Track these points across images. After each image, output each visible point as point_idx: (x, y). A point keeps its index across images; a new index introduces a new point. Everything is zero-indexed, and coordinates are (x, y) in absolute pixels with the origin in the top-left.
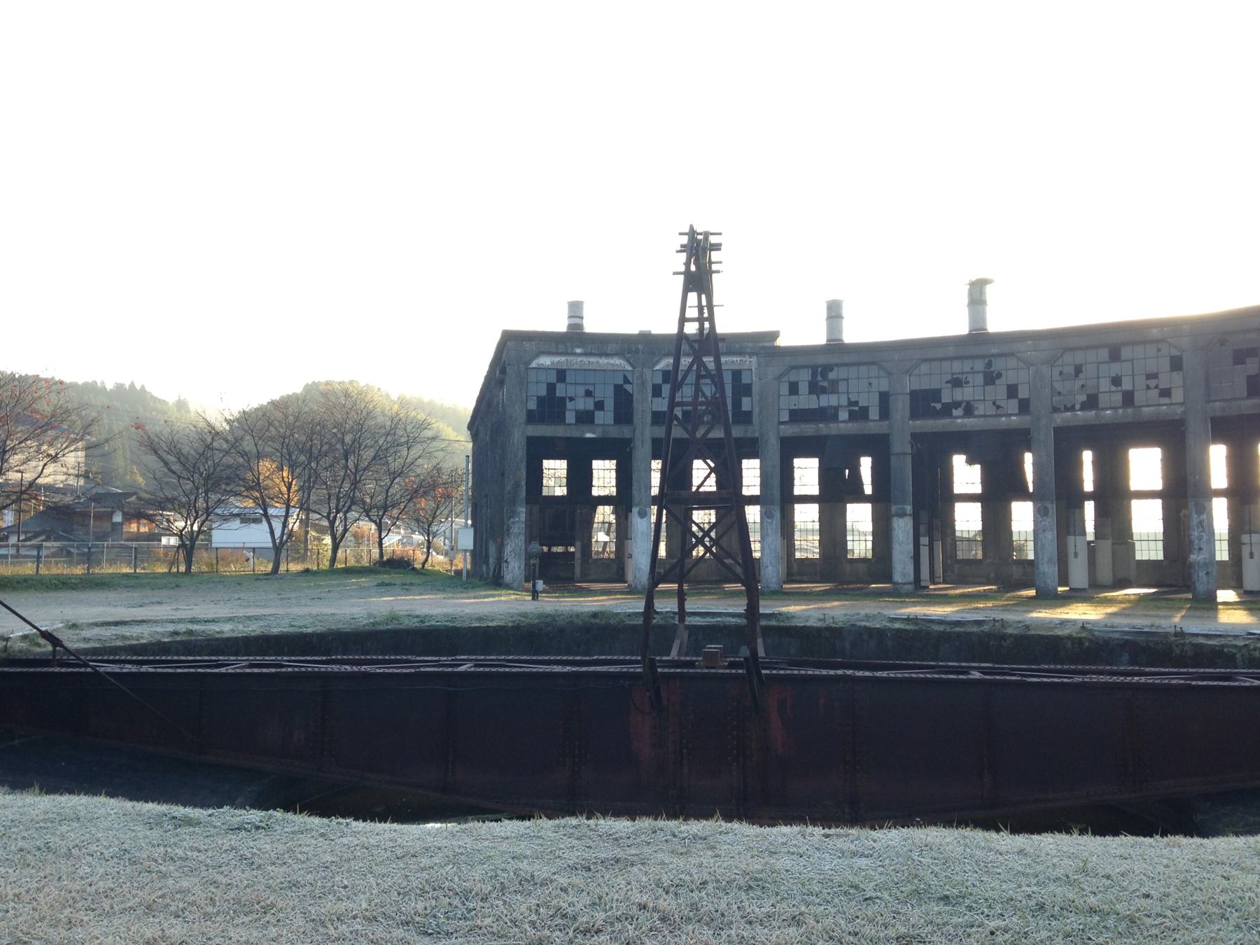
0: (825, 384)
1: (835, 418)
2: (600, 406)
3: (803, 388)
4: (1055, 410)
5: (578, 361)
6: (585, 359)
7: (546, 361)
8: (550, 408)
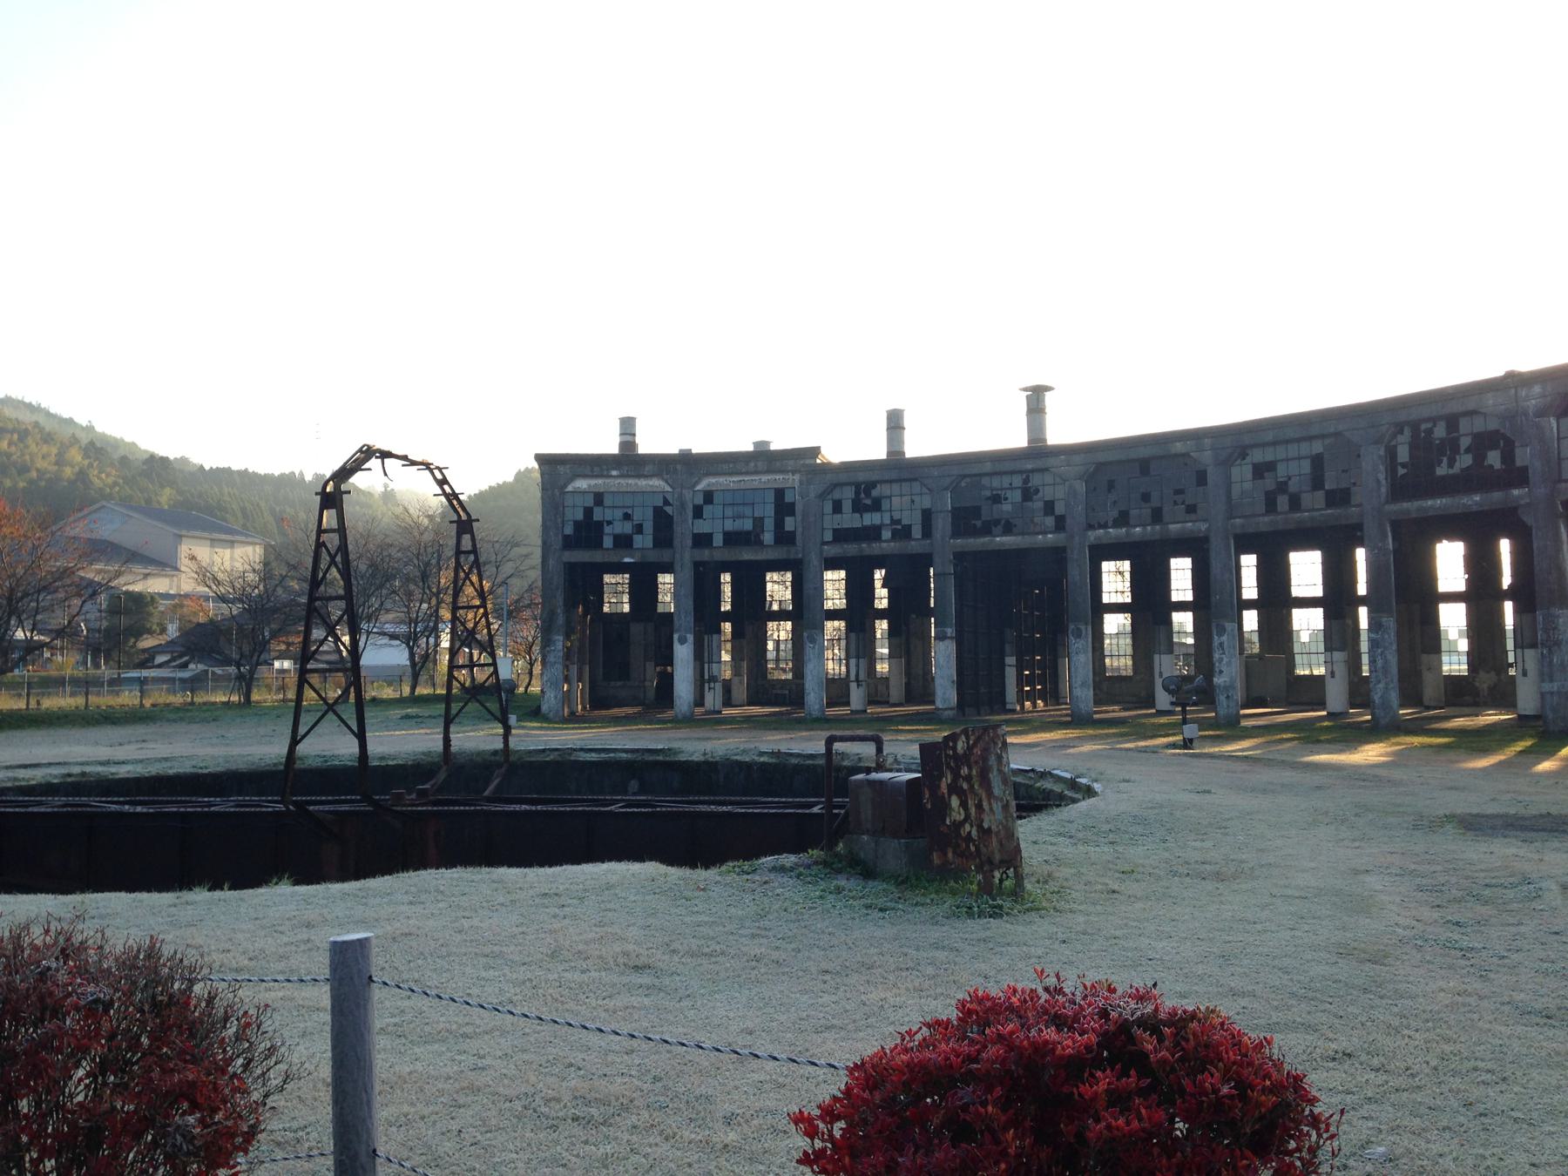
0: (868, 502)
1: (878, 538)
2: (639, 529)
3: (847, 506)
4: (1091, 527)
6: (622, 481)
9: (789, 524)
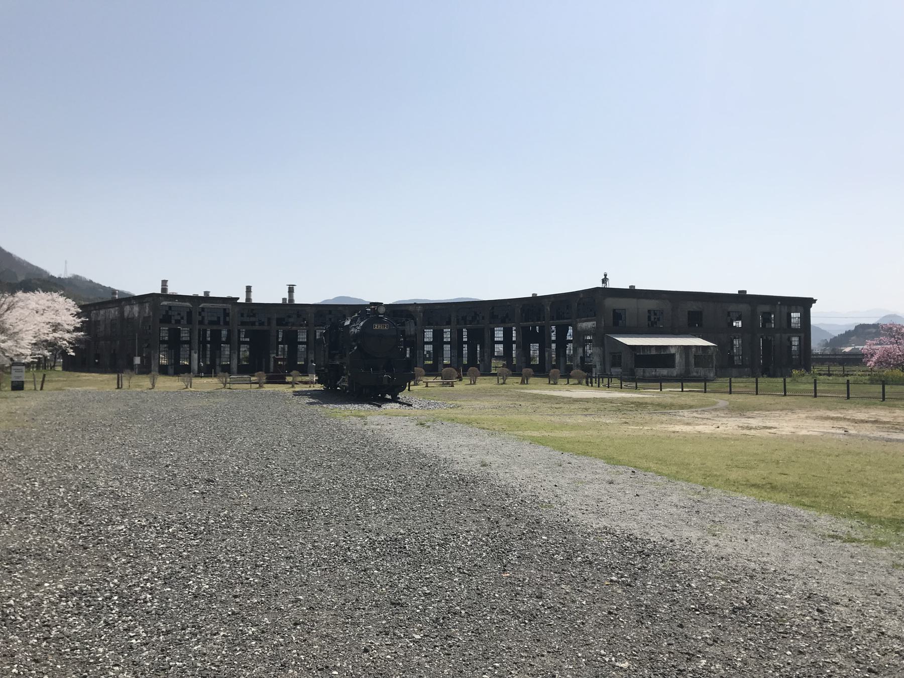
2: (182, 318)
5: (177, 303)
7: (165, 303)
8: (166, 319)
9: (227, 319)
